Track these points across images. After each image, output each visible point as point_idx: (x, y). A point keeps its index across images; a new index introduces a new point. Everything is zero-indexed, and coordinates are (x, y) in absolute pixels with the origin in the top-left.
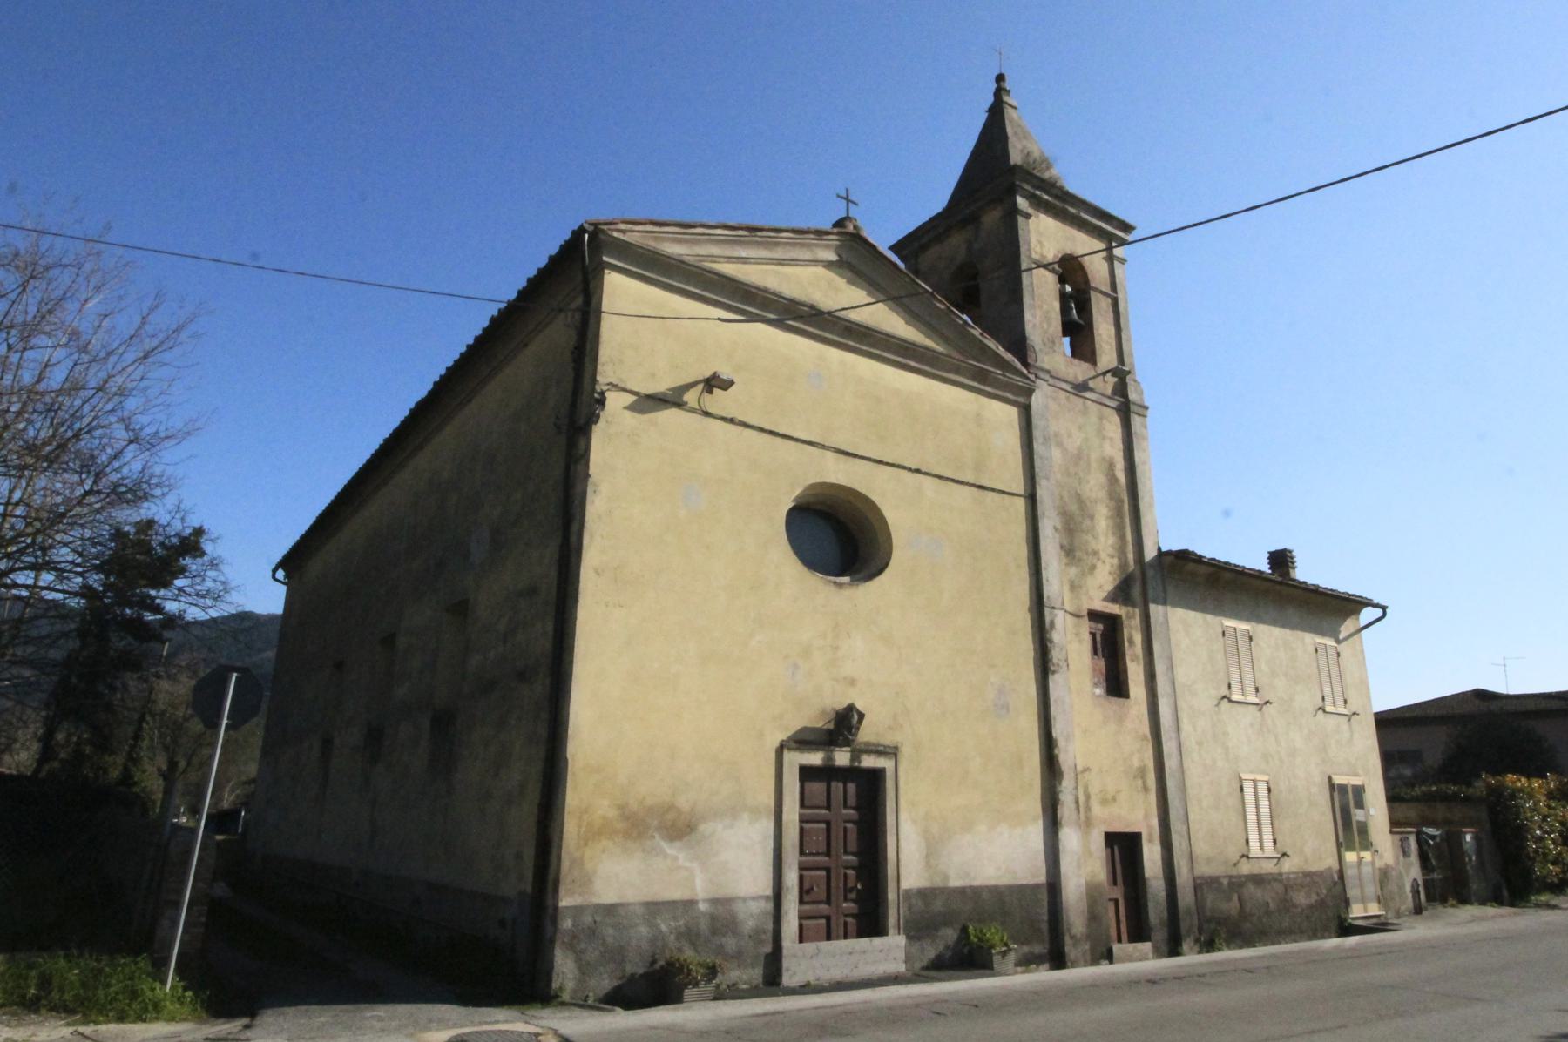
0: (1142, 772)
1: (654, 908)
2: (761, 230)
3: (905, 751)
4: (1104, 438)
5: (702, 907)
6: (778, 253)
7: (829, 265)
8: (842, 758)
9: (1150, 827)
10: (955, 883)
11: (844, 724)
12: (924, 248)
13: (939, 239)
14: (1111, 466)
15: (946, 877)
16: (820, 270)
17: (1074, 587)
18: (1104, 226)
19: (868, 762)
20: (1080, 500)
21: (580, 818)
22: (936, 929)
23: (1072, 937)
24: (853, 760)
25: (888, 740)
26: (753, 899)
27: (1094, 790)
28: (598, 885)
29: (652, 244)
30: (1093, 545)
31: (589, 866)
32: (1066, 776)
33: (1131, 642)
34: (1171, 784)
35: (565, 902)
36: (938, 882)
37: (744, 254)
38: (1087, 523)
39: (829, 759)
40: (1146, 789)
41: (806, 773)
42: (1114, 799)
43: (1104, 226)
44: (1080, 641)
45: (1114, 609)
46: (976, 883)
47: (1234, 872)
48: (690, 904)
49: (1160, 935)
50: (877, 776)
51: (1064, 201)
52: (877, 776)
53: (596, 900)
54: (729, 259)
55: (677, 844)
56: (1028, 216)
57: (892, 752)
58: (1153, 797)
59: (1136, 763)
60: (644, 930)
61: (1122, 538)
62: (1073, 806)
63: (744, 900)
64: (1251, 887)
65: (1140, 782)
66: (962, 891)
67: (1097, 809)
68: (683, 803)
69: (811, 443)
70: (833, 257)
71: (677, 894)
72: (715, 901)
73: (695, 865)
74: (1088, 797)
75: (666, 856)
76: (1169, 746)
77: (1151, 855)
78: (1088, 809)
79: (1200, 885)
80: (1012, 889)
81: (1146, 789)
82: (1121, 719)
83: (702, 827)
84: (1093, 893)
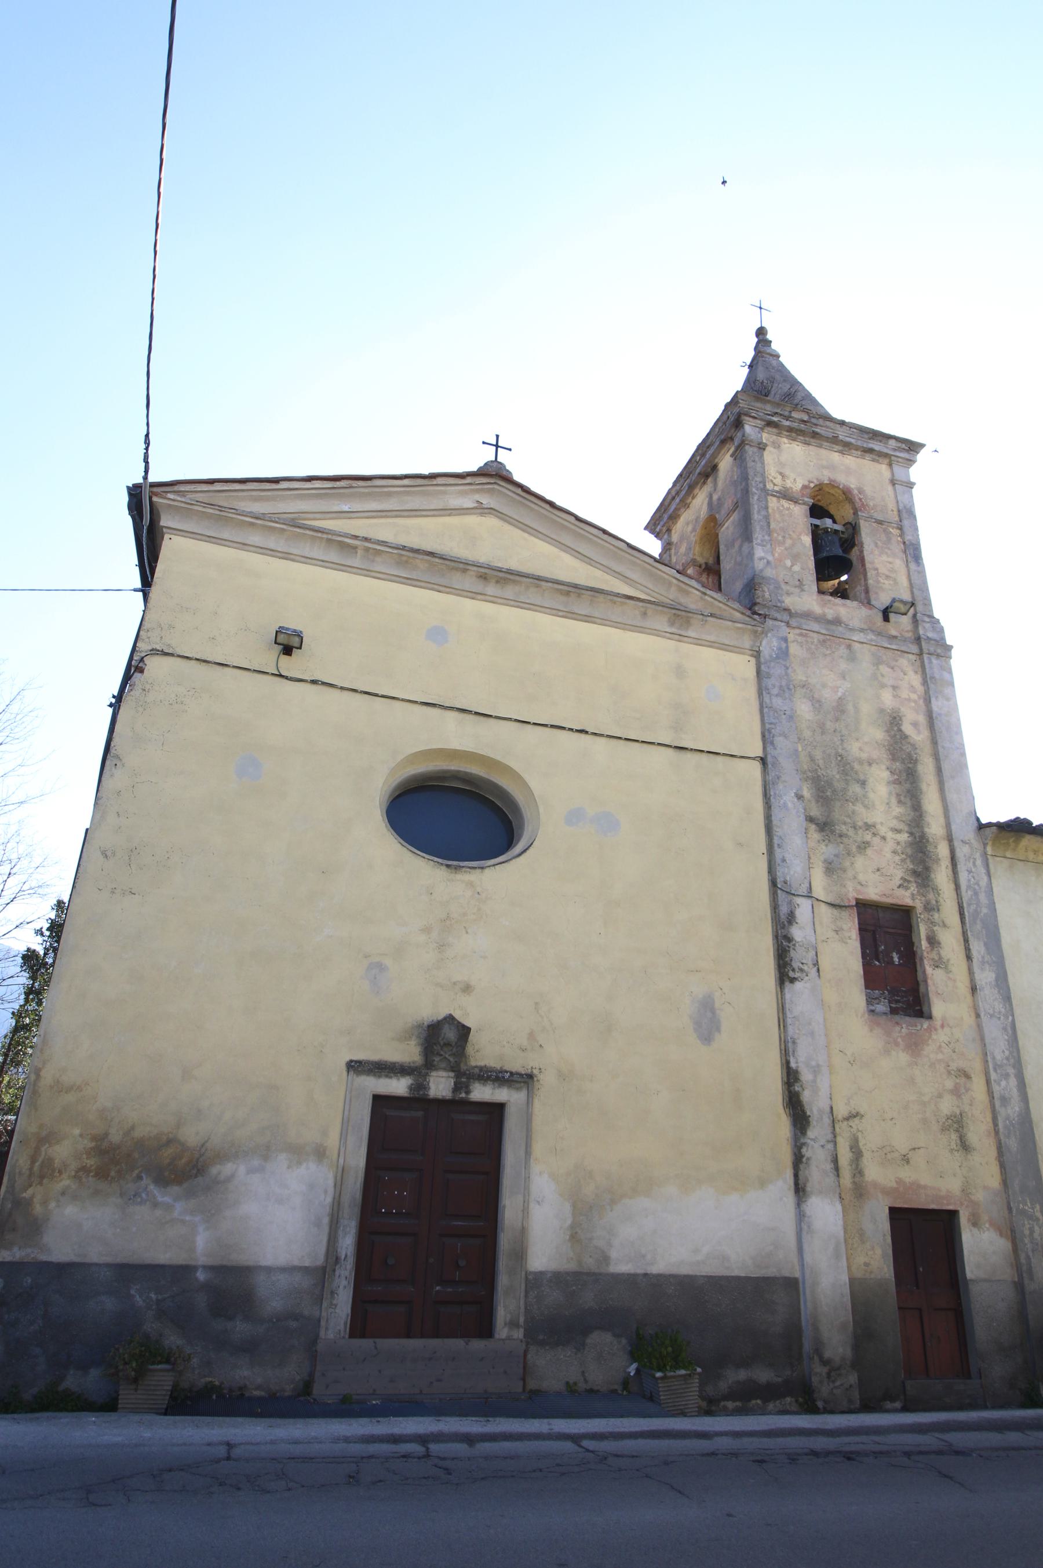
1: (128, 1272)
3: (547, 1080)
4: (883, 686)
5: (201, 1276)
8: (440, 1085)
10: (621, 1265)
11: (444, 1040)
12: (674, 517)
13: (685, 504)
14: (894, 722)
15: (606, 1259)
17: (830, 869)
19: (481, 1093)
20: (845, 765)
21: (37, 1150)
22: (586, 1331)
23: (825, 1362)
24: (457, 1088)
25: (516, 1064)
26: (283, 1270)
27: (869, 1142)
28: (50, 1238)
30: (864, 816)
31: (38, 1209)
32: (813, 1121)
36: (590, 1263)
38: (855, 789)
39: (420, 1086)
42: (906, 1160)
44: (843, 941)
46: (654, 1270)
48: (181, 1272)
50: (496, 1111)
52: (496, 1111)
53: (44, 1258)
55: (175, 1189)
56: (762, 447)
57: (525, 1080)
60: (109, 1303)
62: (829, 1166)
63: (269, 1270)
65: (954, 1136)
66: (631, 1280)
68: (191, 1135)
71: (164, 1257)
72: (221, 1270)
73: (197, 1219)
74: (857, 1154)
75: (155, 1205)
78: (858, 1172)
82: (915, 1046)
83: (214, 1170)
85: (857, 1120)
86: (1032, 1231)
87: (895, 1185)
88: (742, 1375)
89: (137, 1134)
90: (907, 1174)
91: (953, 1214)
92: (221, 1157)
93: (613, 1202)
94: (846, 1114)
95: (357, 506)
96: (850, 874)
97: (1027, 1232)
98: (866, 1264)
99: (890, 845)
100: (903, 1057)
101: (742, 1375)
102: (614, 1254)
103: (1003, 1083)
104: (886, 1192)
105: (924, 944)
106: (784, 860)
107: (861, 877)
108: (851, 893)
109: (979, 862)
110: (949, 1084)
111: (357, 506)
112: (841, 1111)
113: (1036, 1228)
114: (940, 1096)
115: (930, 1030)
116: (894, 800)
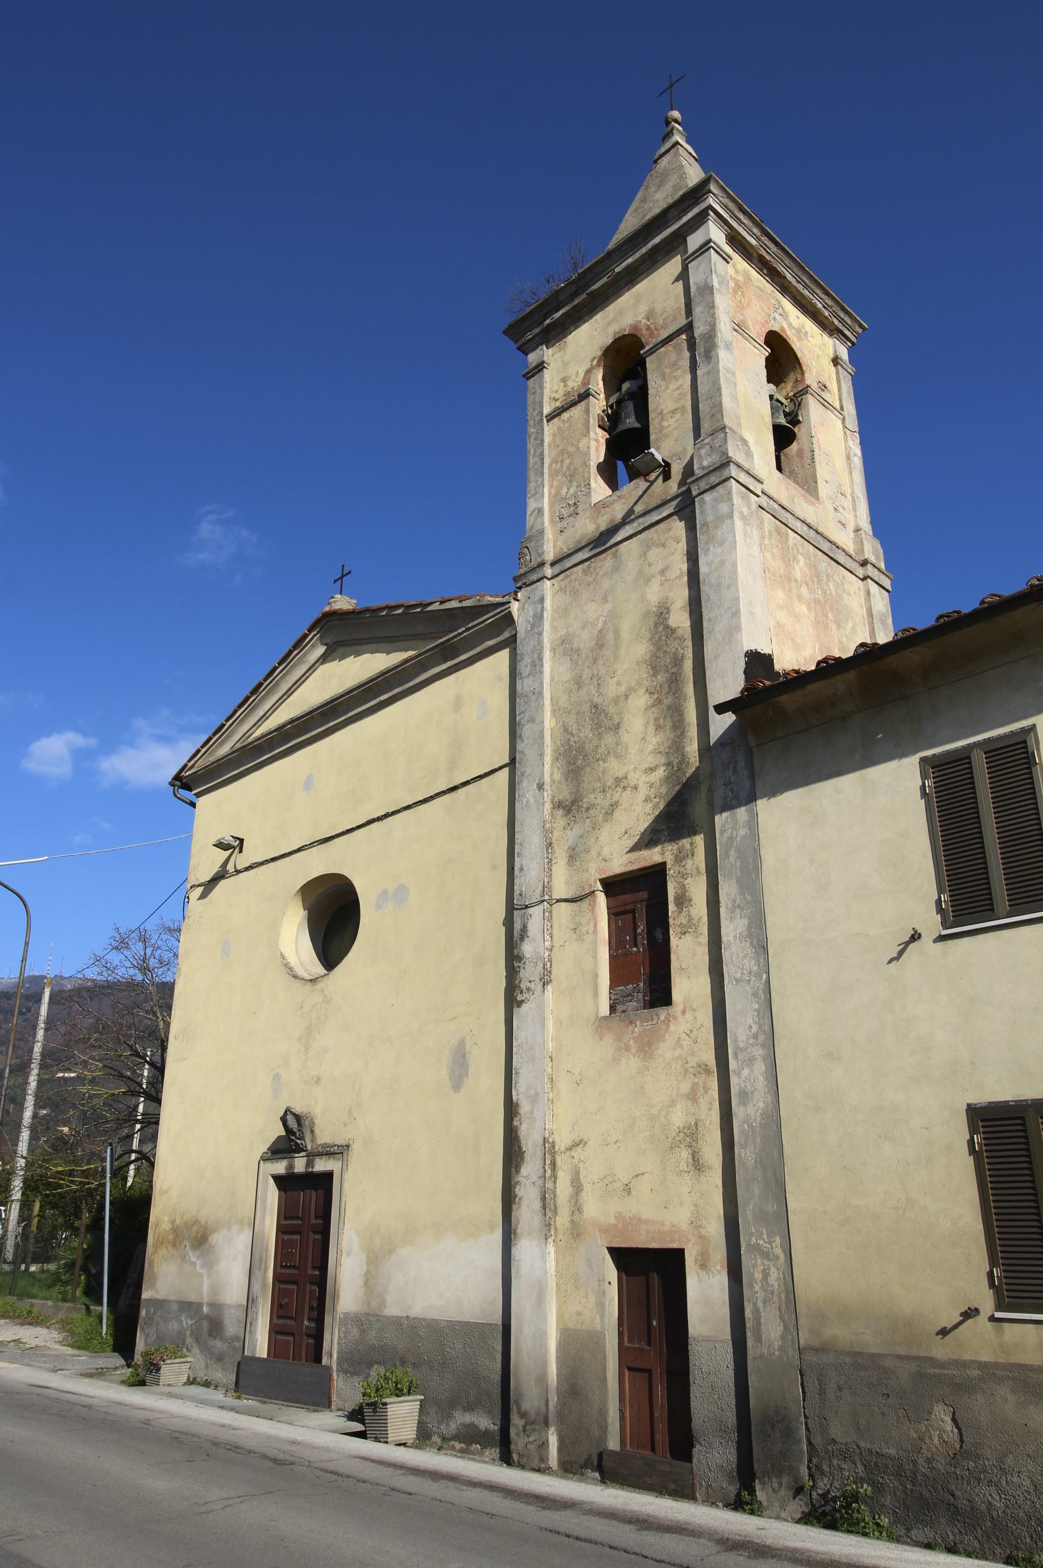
0: (692, 1134)
2: (261, 684)
5: (205, 1309)
6: (284, 687)
7: (324, 659)
8: (300, 1165)
9: (703, 1239)
10: (392, 1310)
14: (662, 614)
15: (383, 1303)
16: (322, 669)
18: (657, 240)
19: (321, 1165)
23: (523, 1415)
24: (308, 1165)
27: (590, 1175)
29: (212, 759)
33: (682, 900)
34: (745, 1155)
35: (145, 1295)
37: (262, 713)
39: (291, 1166)
40: (697, 1165)
41: (278, 1179)
42: (628, 1189)
43: (657, 240)
45: (653, 856)
47: (940, 1350)
49: (714, 1455)
50: (327, 1178)
51: (588, 285)
54: (265, 717)
58: (715, 1178)
59: (678, 1118)
61: (679, 726)
62: (537, 1205)
64: (1006, 1400)
65: (685, 1154)
66: (396, 1322)
67: (593, 1208)
69: (299, 850)
70: (321, 650)
74: (577, 1186)
76: (746, 1076)
77: (705, 1293)
79: (820, 1366)
80: (452, 1325)
81: (697, 1165)
82: (646, 1047)
84: (577, 1347)
85: (579, 1149)
86: (766, 1274)
87: (613, 1221)
88: (468, 1418)
89: (186, 1218)
90: (631, 1207)
91: (678, 1255)
92: (215, 1230)
93: (391, 1251)
94: (569, 1143)
95: (267, 706)
96: (594, 852)
97: (758, 1276)
98: (579, 1314)
99: (643, 791)
100: (632, 1063)
101: (468, 1418)
102: (390, 1298)
103: (745, 1072)
104: (605, 1230)
105: (672, 907)
106: (521, 869)
107: (606, 851)
108: (594, 873)
109: (741, 764)
110: (685, 1087)
111: (267, 706)
112: (562, 1141)
113: (773, 1270)
114: (672, 1104)
115: (667, 1020)
116: (651, 729)
